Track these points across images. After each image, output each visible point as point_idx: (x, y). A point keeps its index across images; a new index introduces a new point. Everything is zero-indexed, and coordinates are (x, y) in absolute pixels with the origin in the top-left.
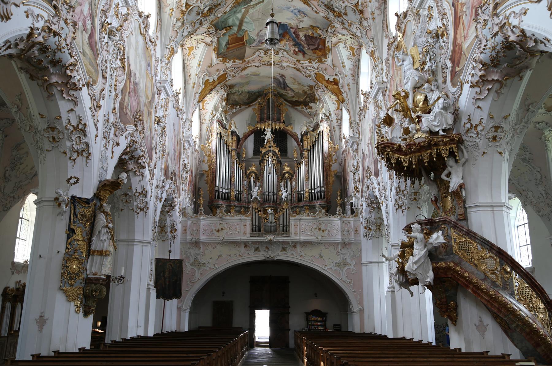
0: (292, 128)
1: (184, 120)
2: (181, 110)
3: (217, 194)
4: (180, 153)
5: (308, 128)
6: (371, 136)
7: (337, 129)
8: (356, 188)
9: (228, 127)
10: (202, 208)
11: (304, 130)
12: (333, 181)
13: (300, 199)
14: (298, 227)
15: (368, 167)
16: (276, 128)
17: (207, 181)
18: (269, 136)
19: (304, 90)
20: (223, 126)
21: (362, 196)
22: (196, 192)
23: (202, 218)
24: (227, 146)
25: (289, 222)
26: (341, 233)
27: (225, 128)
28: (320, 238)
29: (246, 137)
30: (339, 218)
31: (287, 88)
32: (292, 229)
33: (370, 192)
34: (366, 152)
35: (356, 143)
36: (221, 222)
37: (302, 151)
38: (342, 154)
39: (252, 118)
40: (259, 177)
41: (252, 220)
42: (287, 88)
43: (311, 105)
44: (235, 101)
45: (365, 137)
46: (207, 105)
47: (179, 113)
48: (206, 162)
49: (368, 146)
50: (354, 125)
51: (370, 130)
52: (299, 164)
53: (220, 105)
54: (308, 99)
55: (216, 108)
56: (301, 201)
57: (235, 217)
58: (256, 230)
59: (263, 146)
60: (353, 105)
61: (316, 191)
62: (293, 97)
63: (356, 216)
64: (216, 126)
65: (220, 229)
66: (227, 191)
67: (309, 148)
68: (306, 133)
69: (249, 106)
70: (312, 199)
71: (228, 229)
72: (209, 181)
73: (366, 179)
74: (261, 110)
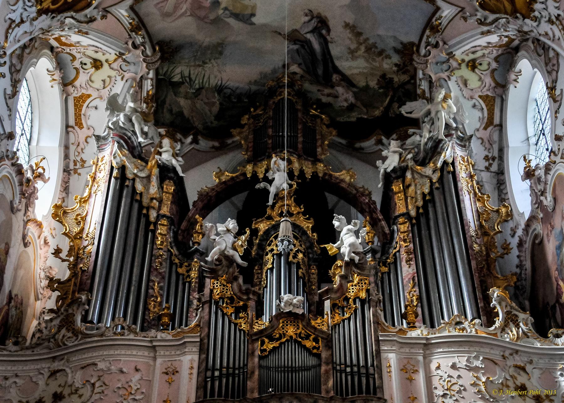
14: (420, 378)
19: (383, 76)
20: (137, 153)
31: (335, 77)
41: (203, 349)
44: (181, 114)
62: (351, 108)
67: (413, 213)
68: (399, 173)
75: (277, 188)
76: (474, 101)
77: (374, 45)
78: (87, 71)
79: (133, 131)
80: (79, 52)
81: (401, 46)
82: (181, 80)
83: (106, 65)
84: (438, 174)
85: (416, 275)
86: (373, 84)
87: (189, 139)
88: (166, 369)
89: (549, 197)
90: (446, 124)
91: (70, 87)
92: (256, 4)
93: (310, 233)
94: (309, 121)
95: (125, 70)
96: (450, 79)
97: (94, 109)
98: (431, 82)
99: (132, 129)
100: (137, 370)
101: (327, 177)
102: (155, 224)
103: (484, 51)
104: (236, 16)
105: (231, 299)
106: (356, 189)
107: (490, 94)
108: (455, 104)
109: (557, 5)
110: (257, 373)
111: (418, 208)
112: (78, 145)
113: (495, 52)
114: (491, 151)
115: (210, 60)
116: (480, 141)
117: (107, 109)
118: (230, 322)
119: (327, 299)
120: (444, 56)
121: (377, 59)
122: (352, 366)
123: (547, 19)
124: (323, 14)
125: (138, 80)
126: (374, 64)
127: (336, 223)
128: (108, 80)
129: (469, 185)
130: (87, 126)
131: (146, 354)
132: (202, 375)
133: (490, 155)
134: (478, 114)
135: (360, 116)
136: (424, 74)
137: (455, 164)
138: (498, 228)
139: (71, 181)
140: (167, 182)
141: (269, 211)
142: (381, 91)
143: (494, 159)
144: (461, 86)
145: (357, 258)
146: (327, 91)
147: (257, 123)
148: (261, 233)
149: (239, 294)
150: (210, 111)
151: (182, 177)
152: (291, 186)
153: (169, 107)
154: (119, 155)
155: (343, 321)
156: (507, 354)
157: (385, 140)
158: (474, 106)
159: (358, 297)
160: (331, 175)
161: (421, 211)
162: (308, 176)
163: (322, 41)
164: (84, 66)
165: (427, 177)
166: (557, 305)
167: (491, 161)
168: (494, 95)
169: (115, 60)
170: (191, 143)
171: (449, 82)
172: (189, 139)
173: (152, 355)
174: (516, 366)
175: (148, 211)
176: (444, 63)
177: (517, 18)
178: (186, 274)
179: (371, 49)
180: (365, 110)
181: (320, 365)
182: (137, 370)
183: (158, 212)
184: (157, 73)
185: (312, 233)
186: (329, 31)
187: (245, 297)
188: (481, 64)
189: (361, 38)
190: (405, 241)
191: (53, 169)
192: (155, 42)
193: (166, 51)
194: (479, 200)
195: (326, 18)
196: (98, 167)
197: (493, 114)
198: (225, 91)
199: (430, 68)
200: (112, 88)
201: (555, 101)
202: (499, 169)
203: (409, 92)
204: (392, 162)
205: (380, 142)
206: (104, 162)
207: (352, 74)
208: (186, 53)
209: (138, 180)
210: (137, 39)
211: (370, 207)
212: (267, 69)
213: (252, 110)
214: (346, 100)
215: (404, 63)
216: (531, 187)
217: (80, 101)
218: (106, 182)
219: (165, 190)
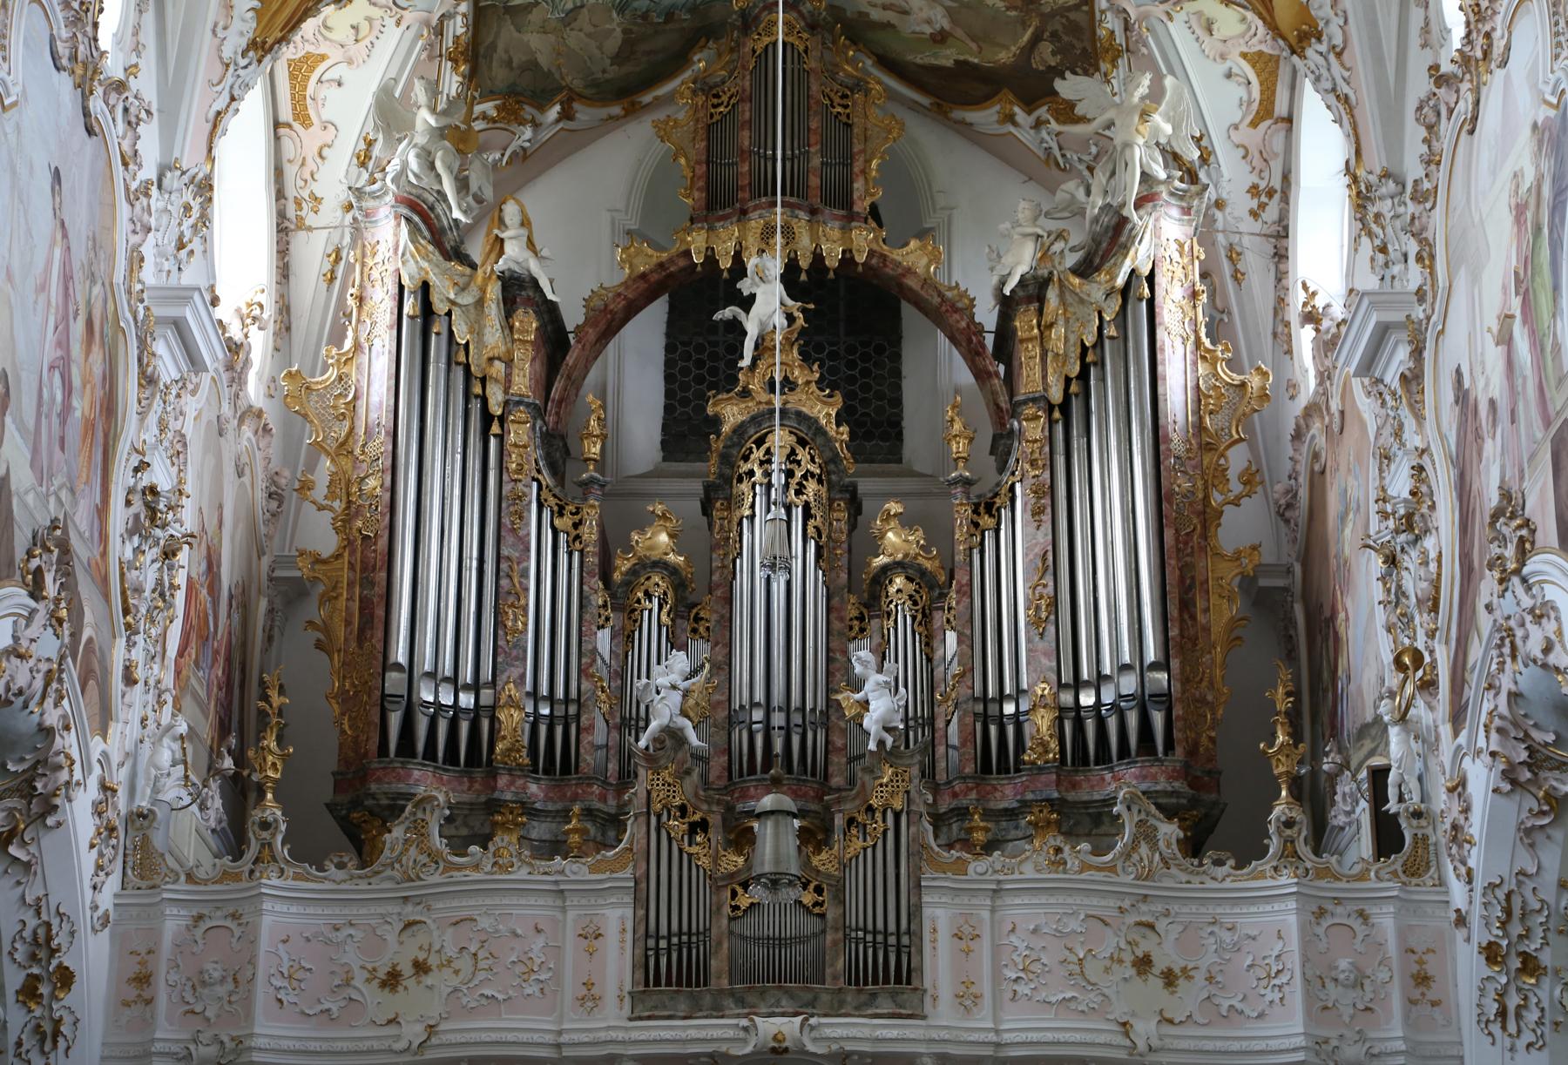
0: (935, 258)
1: (148, 172)
2: (120, 86)
3: (395, 720)
4: (109, 407)
5: (1045, 255)
6: (1529, 261)
7: (1255, 262)
8: (1409, 661)
9: (476, 250)
10: (272, 809)
11: (1021, 262)
12: (1234, 623)
13: (997, 757)
14: (984, 947)
15: (1506, 495)
16: (818, 258)
17: (326, 629)
18: (768, 307)
21: (1457, 717)
22: (238, 710)
23: (271, 882)
24: (473, 382)
25: (915, 912)
26: (1309, 996)
27: (456, 254)
28: (1145, 1029)
29: (609, 319)
30: (1287, 881)
32: (939, 964)
33: (1528, 678)
34: (1489, 383)
35: (1400, 334)
37: (1004, 416)
38: (1298, 436)
39: (653, 196)
40: (700, 605)
41: (640, 899)
43: (1068, 87)
44: (532, 66)
45: (1475, 278)
46: (329, 92)
47: (97, 104)
48: (320, 492)
49: (1505, 339)
50: (1385, 207)
51: (1519, 210)
52: (988, 507)
53: (420, 93)
54: (1046, 48)
55: (390, 114)
56: (1003, 768)
57: (523, 873)
58: (673, 971)
59: (726, 380)
60: (1379, 60)
61: (1108, 696)
62: (940, 38)
63: (1415, 869)
64: (389, 233)
65: (406, 969)
66: (467, 700)
67: (1056, 395)
68: (1034, 290)
69: (633, 111)
70: (1081, 758)
71: (465, 964)
72: (341, 632)
73: (1488, 585)
74: (715, 133)
75: (762, 324)
76: (1228, 64)
79: (439, 192)
84: (1116, 302)
87: (554, 112)
90: (1143, 173)
93: (832, 429)
94: (837, 100)
96: (1171, 19)
98: (1126, 21)
99: (436, 187)
101: (874, 261)
102: (502, 420)
105: (683, 810)
106: (940, 294)
109: (1346, 74)
110: (726, 945)
111: (1068, 381)
114: (1266, 174)
116: (1241, 152)
118: (681, 851)
122: (875, 932)
125: (434, 22)
131: (550, 901)
132: (641, 944)
133: (1263, 185)
134: (1236, 91)
135: (962, 58)
140: (520, 311)
142: (1013, 13)
143: (1270, 193)
144: (1199, 31)
147: (715, 106)
148: (726, 428)
150: (600, 48)
152: (790, 318)
155: (865, 849)
156: (1126, 904)
158: (1229, 75)
160: (884, 257)
161: (1074, 388)
167: (1264, 199)
170: (558, 121)
171: (1169, 24)
172: (554, 112)
173: (559, 903)
174: (1139, 924)
178: (574, 533)
180: (974, 46)
181: (824, 932)
183: (506, 392)
185: (838, 425)
187: (705, 807)
190: (1033, 463)
194: (1204, 358)
196: (366, 270)
197: (1274, 92)
205: (1010, 118)
211: (970, 341)
214: (929, 22)
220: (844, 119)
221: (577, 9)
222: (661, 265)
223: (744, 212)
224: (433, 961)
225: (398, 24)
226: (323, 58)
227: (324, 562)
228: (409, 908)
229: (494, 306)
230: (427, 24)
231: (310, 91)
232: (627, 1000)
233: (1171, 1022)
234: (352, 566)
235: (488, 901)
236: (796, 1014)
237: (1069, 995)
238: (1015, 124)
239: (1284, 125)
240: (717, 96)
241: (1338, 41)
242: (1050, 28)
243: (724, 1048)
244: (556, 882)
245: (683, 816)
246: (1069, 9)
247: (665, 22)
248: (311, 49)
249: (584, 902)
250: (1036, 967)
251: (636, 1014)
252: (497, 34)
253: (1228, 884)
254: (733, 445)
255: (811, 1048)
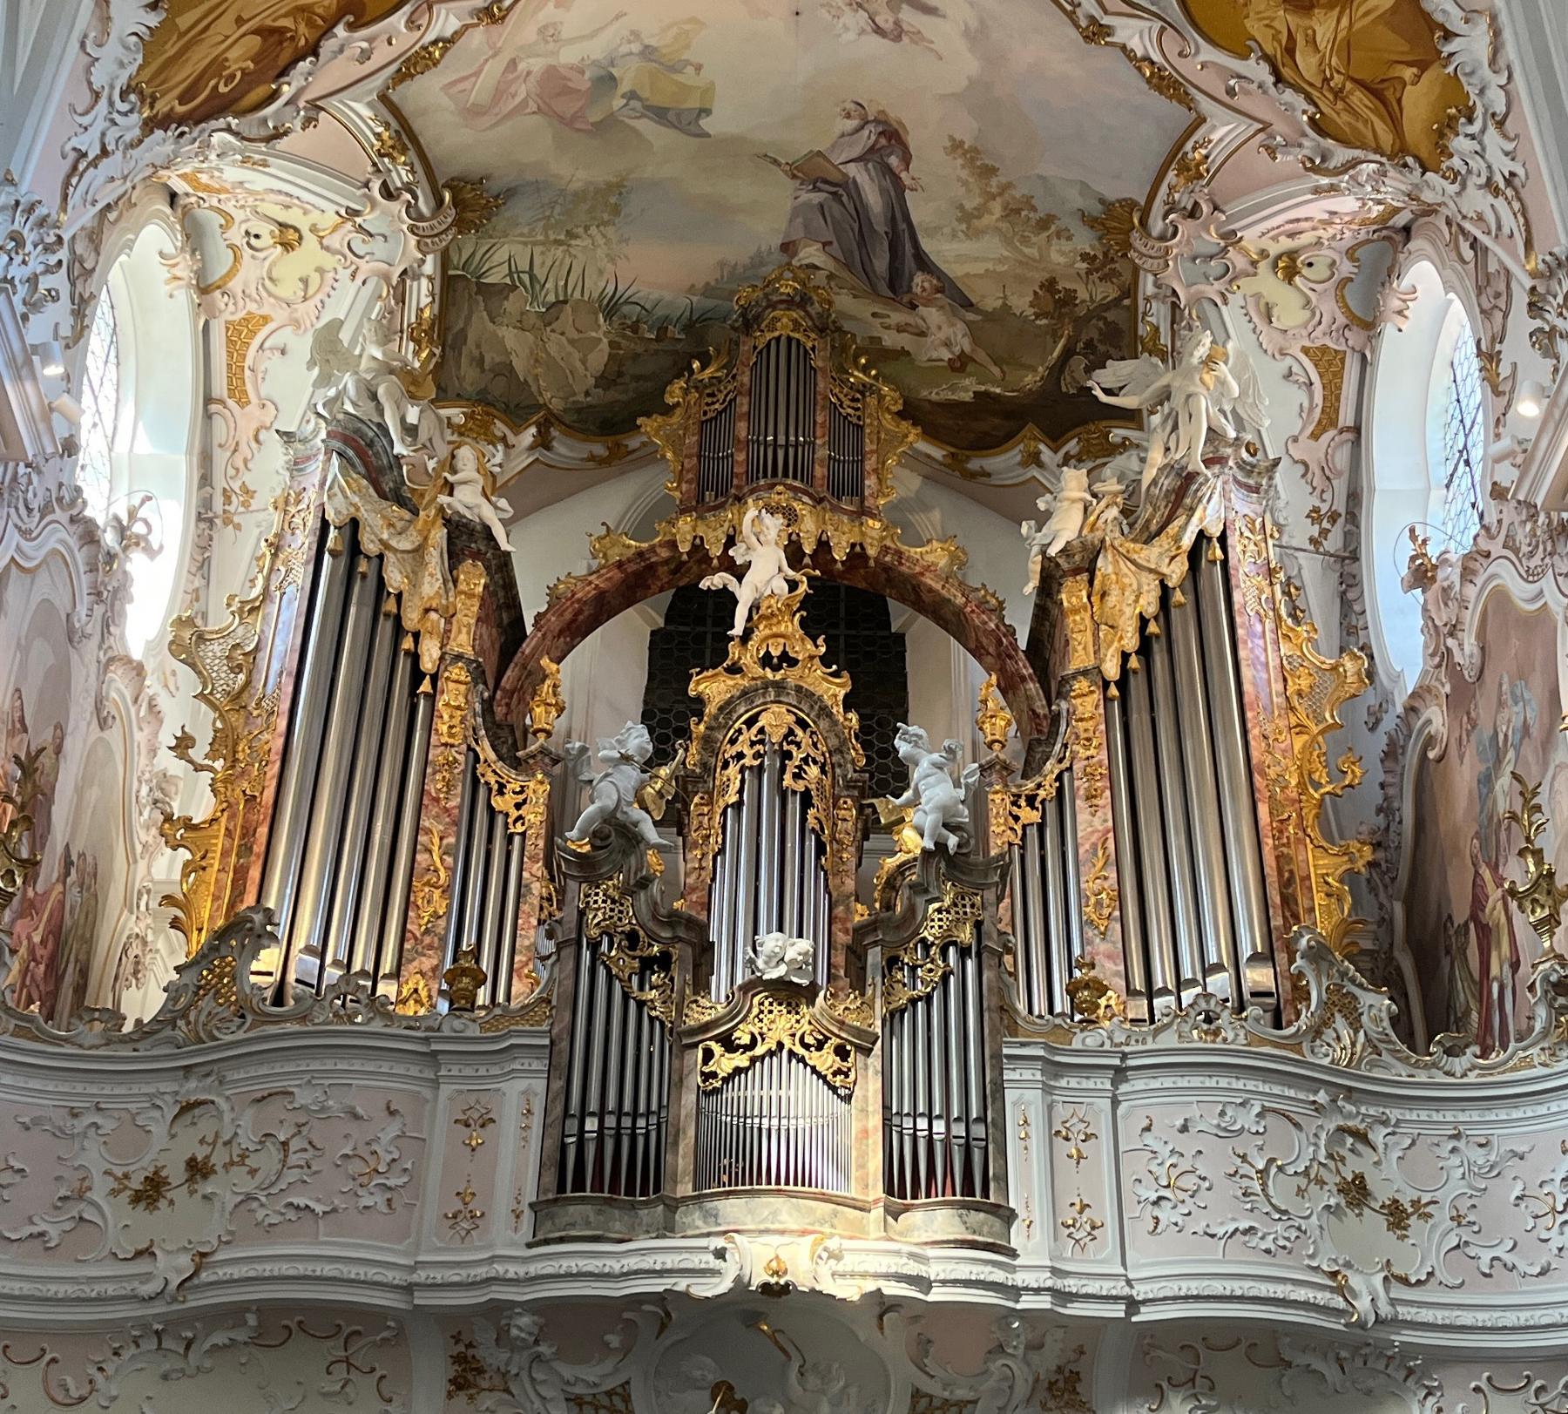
19: (1050, 285)
29: (580, 619)
31: (920, 281)
36: (193, 1089)
41: (558, 1063)
42: (920, 281)
44: (506, 370)
46: (273, 362)
62: (961, 364)
65: (176, 1173)
67: (1112, 670)
71: (268, 1160)
76: (1289, 361)
77: (1029, 204)
78: (260, 255)
79: (379, 425)
80: (242, 207)
81: (1100, 207)
82: (508, 280)
83: (310, 240)
85: (1111, 835)
86: (1021, 303)
87: (529, 435)
88: (464, 1112)
89: (1470, 643)
90: (1209, 429)
91: (217, 293)
92: (713, 83)
93: (838, 710)
94: (847, 403)
95: (361, 253)
97: (278, 354)
98: (1175, 306)
99: (377, 419)
100: (392, 1113)
102: (435, 679)
103: (1321, 232)
104: (660, 114)
105: (632, 938)
107: (1331, 345)
108: (1235, 373)
111: (1125, 656)
112: (236, 450)
113: (1348, 234)
115: (587, 228)
116: (1301, 469)
117: (311, 364)
118: (626, 997)
119: (875, 943)
120: (1213, 238)
121: (1034, 239)
123: (1483, 180)
124: (893, 114)
125: (395, 280)
126: (1027, 251)
127: (903, 747)
128: (315, 280)
129: (1263, 597)
130: (259, 398)
131: (414, 1071)
132: (555, 1132)
133: (1324, 508)
135: (983, 388)
136: (1157, 285)
137: (1230, 541)
138: (1333, 717)
139: (214, 544)
141: (734, 649)
145: (953, 841)
146: (897, 317)
148: (711, 709)
149: (651, 925)
150: (584, 362)
151: (508, 554)
152: (793, 585)
153: (476, 353)
154: (343, 492)
156: (1322, 1097)
157: (1046, 454)
159: (954, 943)
160: (899, 553)
161: (1134, 663)
162: (839, 555)
163: (888, 183)
164: (253, 241)
165: (1151, 571)
166: (1472, 926)
167: (1325, 525)
168: (1343, 348)
169: (335, 228)
170: (532, 448)
171: (1223, 308)
175: (416, 642)
176: (1211, 257)
177: (1405, 165)
178: (514, 814)
179: (1018, 211)
180: (996, 371)
182: (392, 1113)
184: (445, 261)
185: (847, 709)
186: (907, 159)
187: (666, 934)
188: (1310, 265)
189: (994, 181)
191: (169, 522)
192: (441, 182)
193: (467, 204)
194: (1286, 636)
195: (900, 123)
197: (1338, 399)
198: (626, 309)
199: (1172, 269)
200: (326, 299)
201: (1497, 393)
202: (1345, 547)
203: (1116, 334)
204: (1065, 528)
205: (1034, 459)
206: (303, 506)
207: (967, 275)
208: (520, 210)
209: (390, 557)
210: (394, 174)
212: (737, 252)
213: (696, 365)
215: (1105, 254)
216: (1425, 609)
217: (240, 335)
218: (307, 563)
219: (462, 587)
220: (855, 420)
221: (561, 303)
222: (640, 554)
223: (739, 499)
224: (219, 1158)
225: (353, 276)
226: (266, 319)
227: (196, 828)
228: (192, 1084)
229: (436, 553)
230: (386, 278)
231: (248, 362)
232: (528, 1216)
233: (1404, 1281)
234: (229, 833)
235: (315, 1066)
236: (804, 1233)
237: (1244, 1225)
238: (1040, 465)
239: (1349, 436)
240: (712, 395)
241: (1500, 108)
242: (1084, 337)
243: (681, 1284)
244: (426, 1040)
245: (633, 947)
246: (1107, 307)
247: (658, 340)
248: (252, 307)
249: (469, 1071)
250: (1189, 1182)
251: (540, 1236)
252: (468, 319)
253: (1472, 1078)
254: (719, 727)
255: (828, 1286)
